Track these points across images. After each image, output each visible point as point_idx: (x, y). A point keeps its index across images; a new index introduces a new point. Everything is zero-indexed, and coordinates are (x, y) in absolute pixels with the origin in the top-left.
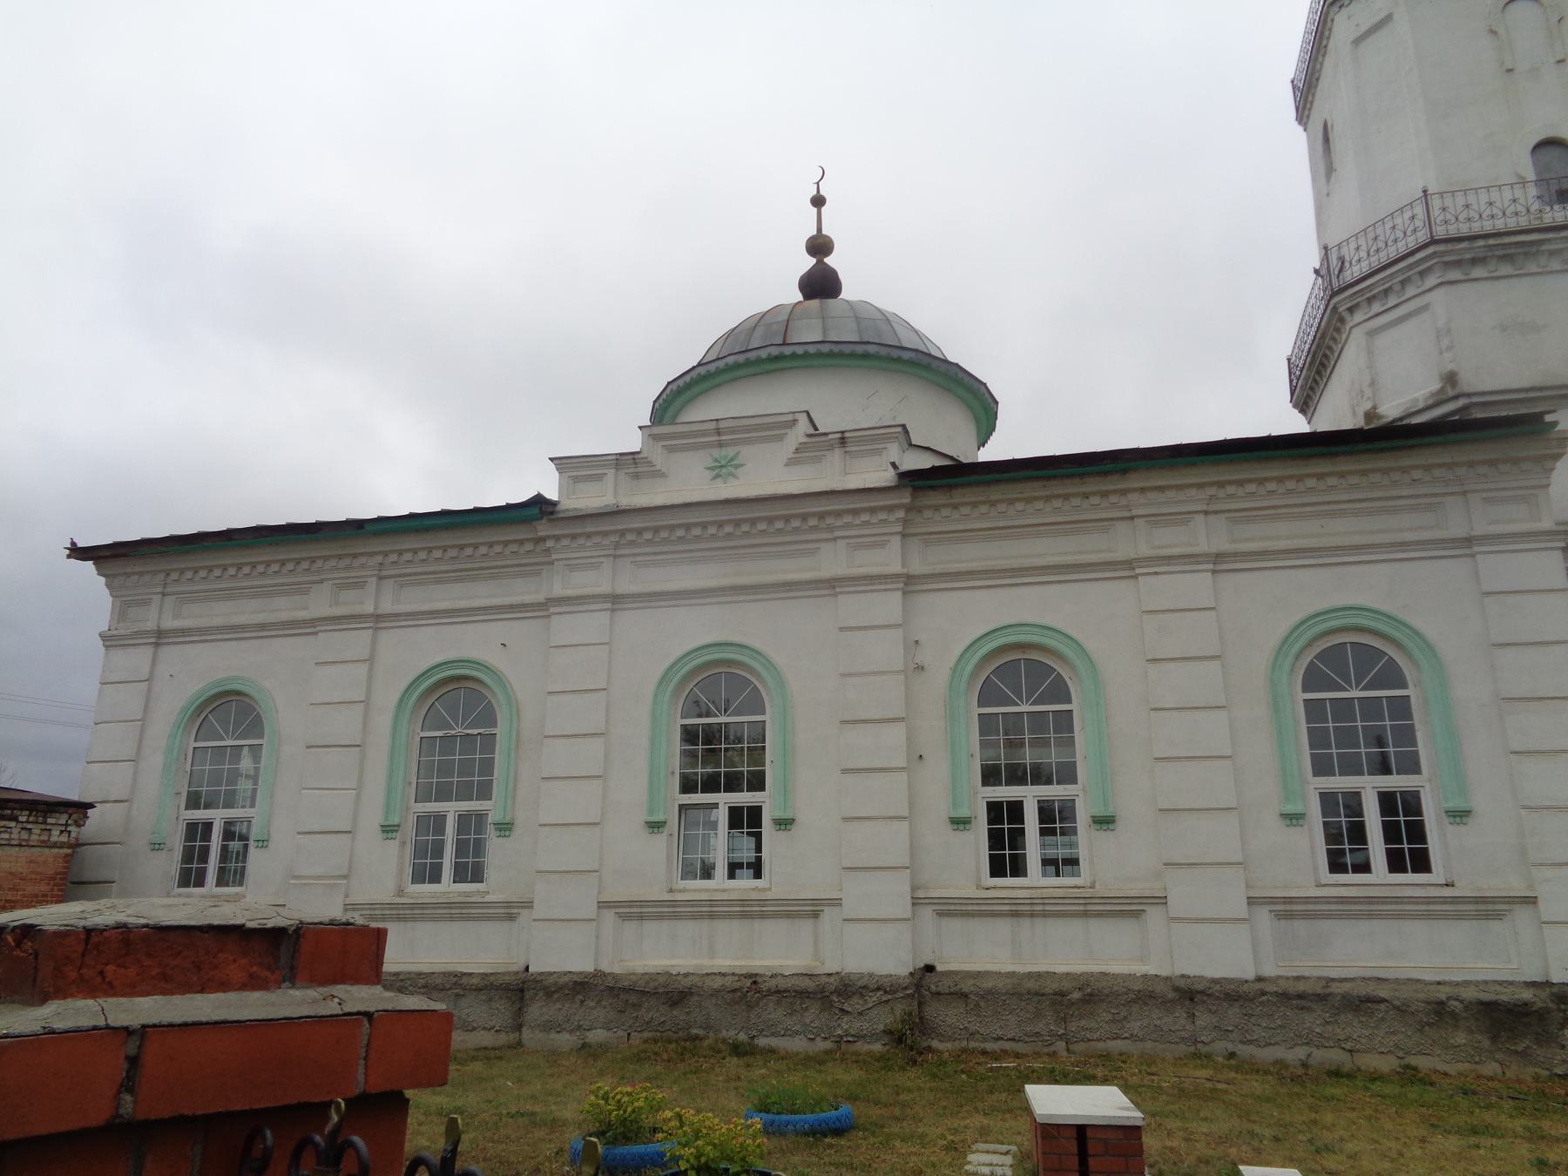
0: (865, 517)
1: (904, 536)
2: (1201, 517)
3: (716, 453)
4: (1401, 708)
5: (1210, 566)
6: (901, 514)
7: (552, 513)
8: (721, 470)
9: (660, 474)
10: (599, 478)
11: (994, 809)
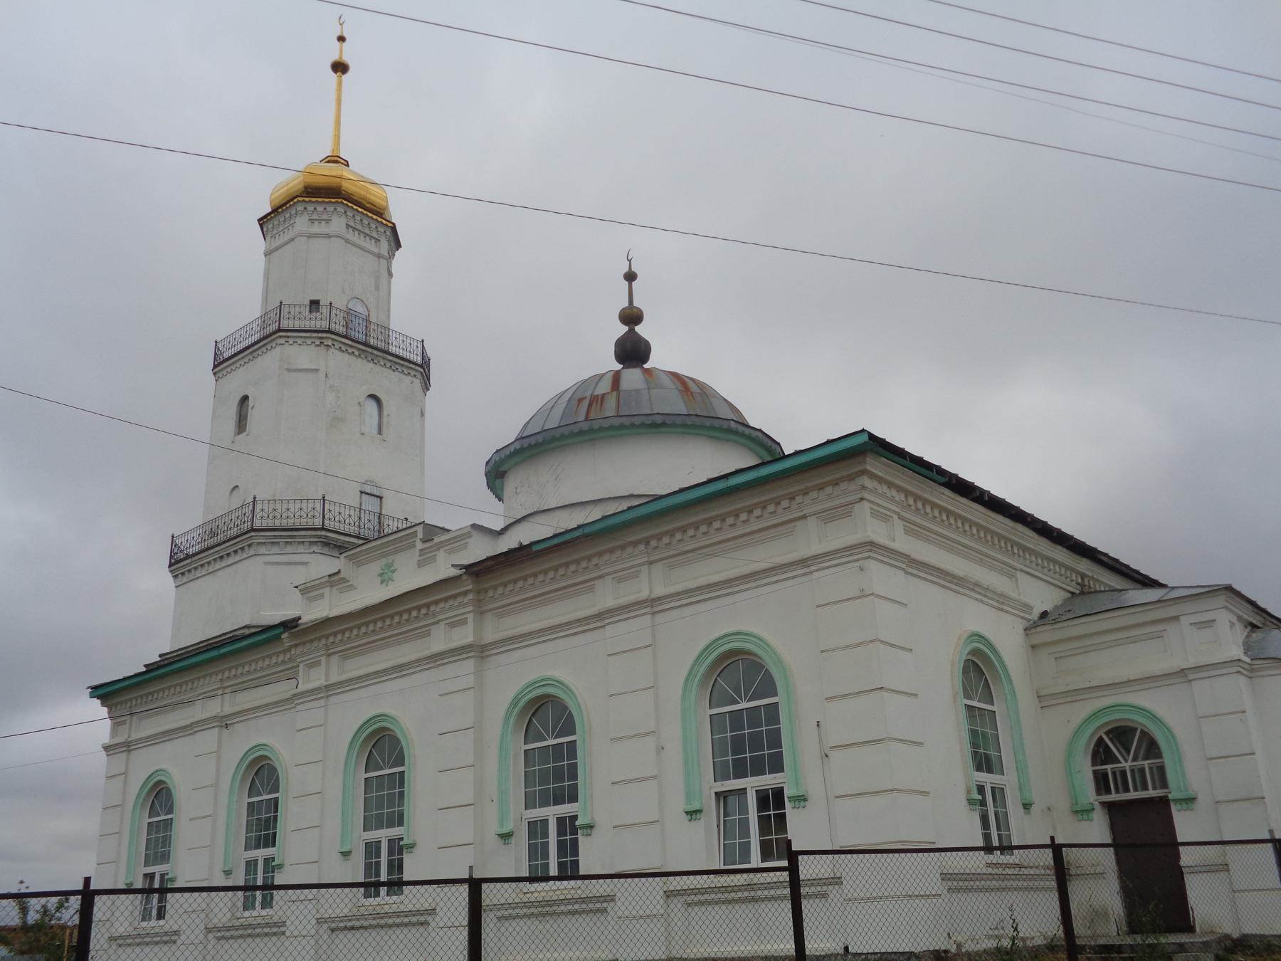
0: (451, 602)
1: (480, 612)
2: (645, 569)
3: (383, 562)
4: (773, 712)
5: (648, 610)
6: (470, 596)
7: (296, 626)
8: (384, 578)
9: (352, 587)
10: (321, 596)
11: (532, 825)
